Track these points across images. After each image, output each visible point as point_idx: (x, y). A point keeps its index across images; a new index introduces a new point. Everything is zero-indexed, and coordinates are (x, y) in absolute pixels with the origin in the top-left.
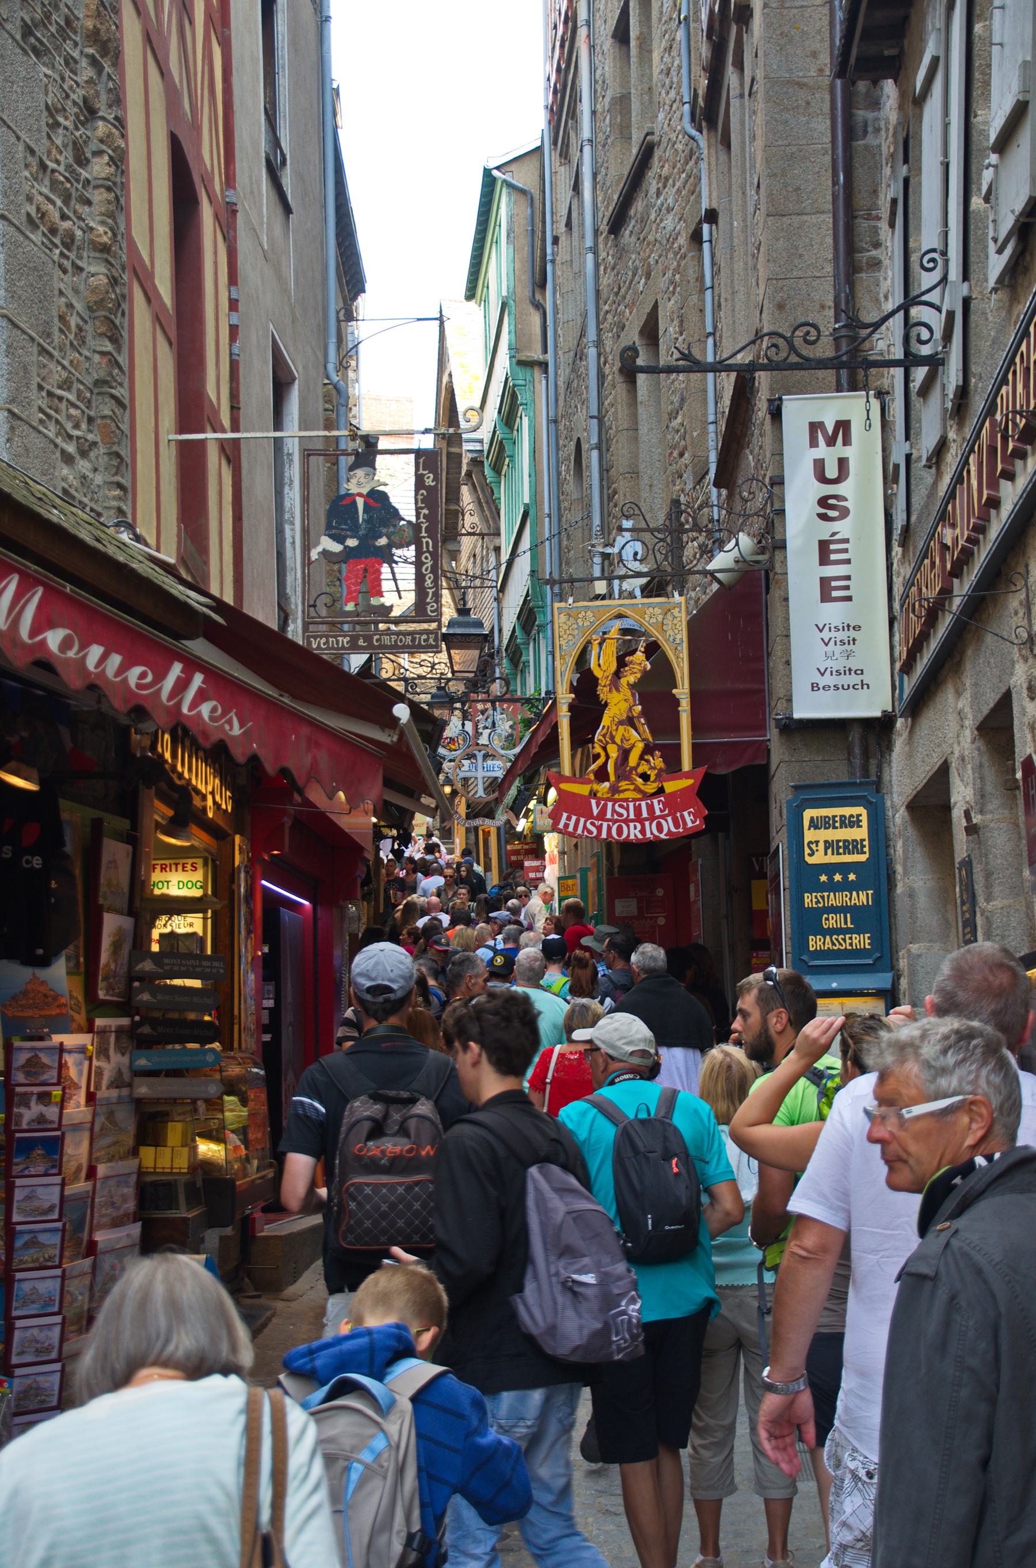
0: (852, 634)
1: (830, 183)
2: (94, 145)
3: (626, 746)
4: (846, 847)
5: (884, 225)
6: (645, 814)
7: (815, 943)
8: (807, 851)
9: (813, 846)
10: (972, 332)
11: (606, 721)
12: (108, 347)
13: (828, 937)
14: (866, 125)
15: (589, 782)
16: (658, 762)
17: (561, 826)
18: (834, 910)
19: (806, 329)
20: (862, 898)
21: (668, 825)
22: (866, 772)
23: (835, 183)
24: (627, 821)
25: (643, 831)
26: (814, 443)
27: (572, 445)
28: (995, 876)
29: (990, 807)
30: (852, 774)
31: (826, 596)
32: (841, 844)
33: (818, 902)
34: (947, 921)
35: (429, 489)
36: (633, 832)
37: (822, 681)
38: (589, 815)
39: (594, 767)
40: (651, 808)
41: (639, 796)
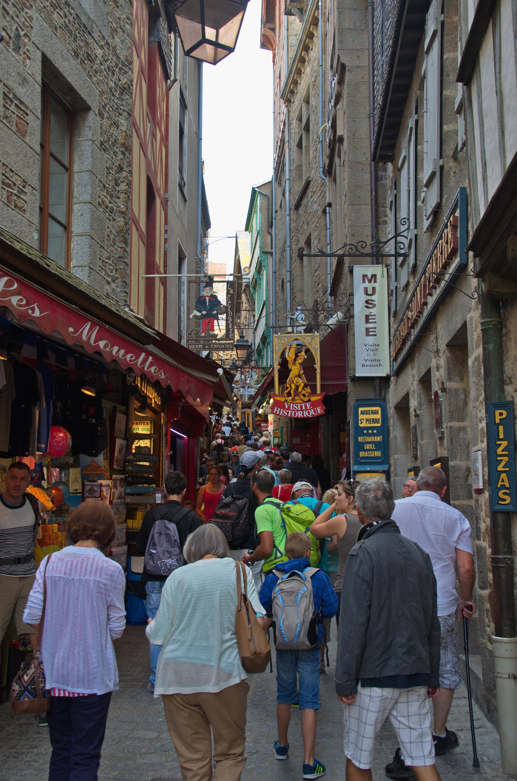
0: (376, 347)
1: (370, 195)
2: (122, 179)
3: (298, 385)
4: (373, 421)
5: (388, 210)
6: (304, 408)
7: (362, 454)
8: (360, 422)
10: (418, 246)
11: (291, 376)
12: (123, 245)
14: (382, 177)
15: (284, 397)
16: (308, 390)
17: (275, 412)
19: (362, 243)
20: (379, 439)
21: (312, 412)
22: (380, 395)
23: (372, 195)
25: (303, 414)
26: (364, 282)
27: (281, 280)
29: (423, 408)
30: (376, 396)
31: (367, 334)
35: (231, 294)
36: (300, 415)
37: (366, 363)
38: (284, 408)
39: (286, 392)
40: (306, 406)
41: (302, 402)
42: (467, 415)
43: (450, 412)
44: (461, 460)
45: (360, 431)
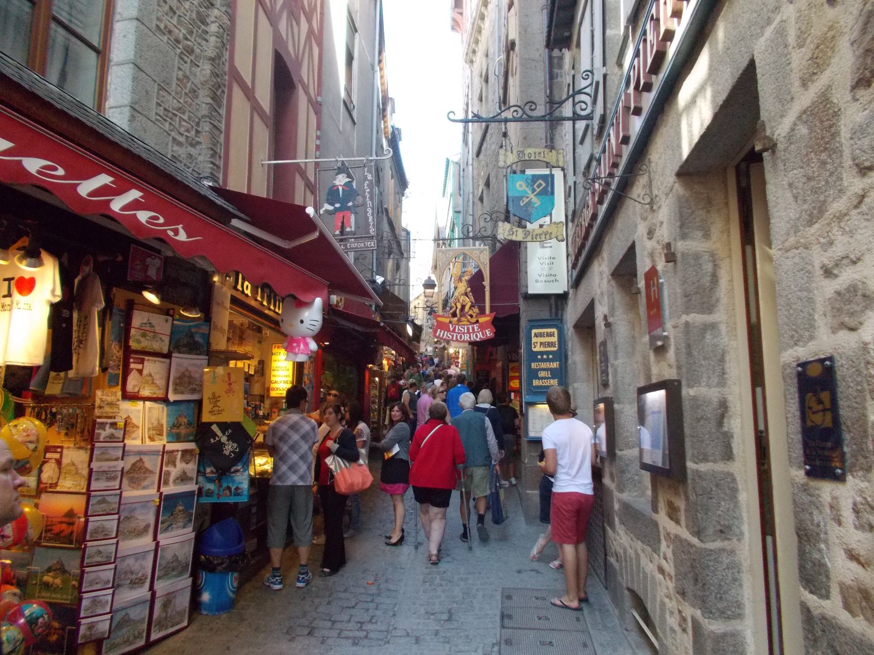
2: (213, 19)
4: (548, 345)
6: (471, 331)
7: (536, 383)
8: (533, 346)
14: (557, 74)
16: (476, 310)
17: (437, 335)
18: (543, 370)
19: (530, 104)
20: (555, 365)
21: (480, 335)
22: (557, 314)
24: (464, 333)
25: (470, 338)
30: (551, 315)
37: (540, 279)
38: (449, 330)
40: (473, 329)
42: (718, 300)
43: (686, 296)
44: (709, 386)
45: (534, 356)
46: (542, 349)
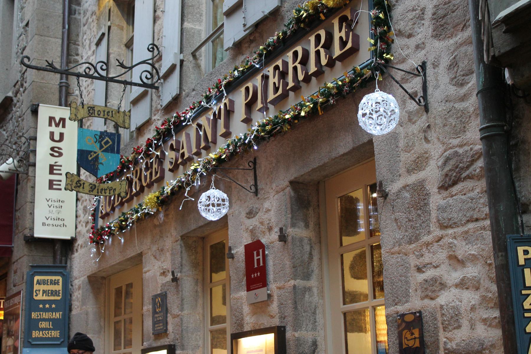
0: (61, 204)
1: (61, 28)
4: (52, 293)
7: (35, 334)
8: (35, 294)
9: (38, 292)
10: (184, 74)
13: (41, 332)
14: (75, 11)
18: (45, 320)
20: (57, 315)
23: (64, 27)
26: (50, 125)
28: (185, 300)
29: (184, 270)
31: (51, 187)
32: (50, 292)
33: (38, 316)
34: (101, 325)
37: (47, 222)
42: (312, 271)
43: (294, 267)
46: (45, 298)
